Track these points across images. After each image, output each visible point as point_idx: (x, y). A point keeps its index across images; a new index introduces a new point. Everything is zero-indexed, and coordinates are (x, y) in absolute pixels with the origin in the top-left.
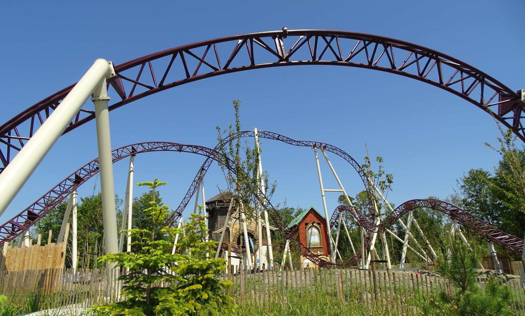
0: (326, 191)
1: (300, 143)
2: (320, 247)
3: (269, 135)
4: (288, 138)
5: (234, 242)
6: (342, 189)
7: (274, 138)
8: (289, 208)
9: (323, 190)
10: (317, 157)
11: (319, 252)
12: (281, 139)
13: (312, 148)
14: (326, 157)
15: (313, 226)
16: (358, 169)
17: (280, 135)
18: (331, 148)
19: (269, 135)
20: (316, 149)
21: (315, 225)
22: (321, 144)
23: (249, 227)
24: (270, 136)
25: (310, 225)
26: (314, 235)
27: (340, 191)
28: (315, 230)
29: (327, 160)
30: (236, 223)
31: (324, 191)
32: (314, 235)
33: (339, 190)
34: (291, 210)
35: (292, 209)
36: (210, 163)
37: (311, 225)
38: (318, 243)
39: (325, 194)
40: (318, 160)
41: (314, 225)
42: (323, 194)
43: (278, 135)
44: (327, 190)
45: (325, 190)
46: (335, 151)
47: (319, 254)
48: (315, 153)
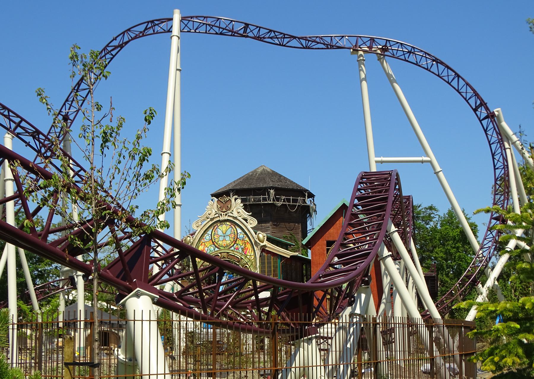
0: (382, 162)
1: (309, 41)
3: (219, 28)
4: (271, 31)
6: (427, 155)
7: (234, 33)
8: (423, 206)
10: (363, 76)
12: (251, 34)
13: (352, 53)
14: (388, 75)
16: (472, 101)
17: (247, 25)
19: (219, 28)
20: (361, 55)
22: (372, 40)
23: (233, 248)
24: (221, 30)
27: (422, 162)
29: (391, 83)
30: (203, 241)
31: (376, 162)
34: (429, 211)
35: (431, 208)
40: (364, 83)
43: (243, 26)
46: (412, 58)
48: (360, 66)
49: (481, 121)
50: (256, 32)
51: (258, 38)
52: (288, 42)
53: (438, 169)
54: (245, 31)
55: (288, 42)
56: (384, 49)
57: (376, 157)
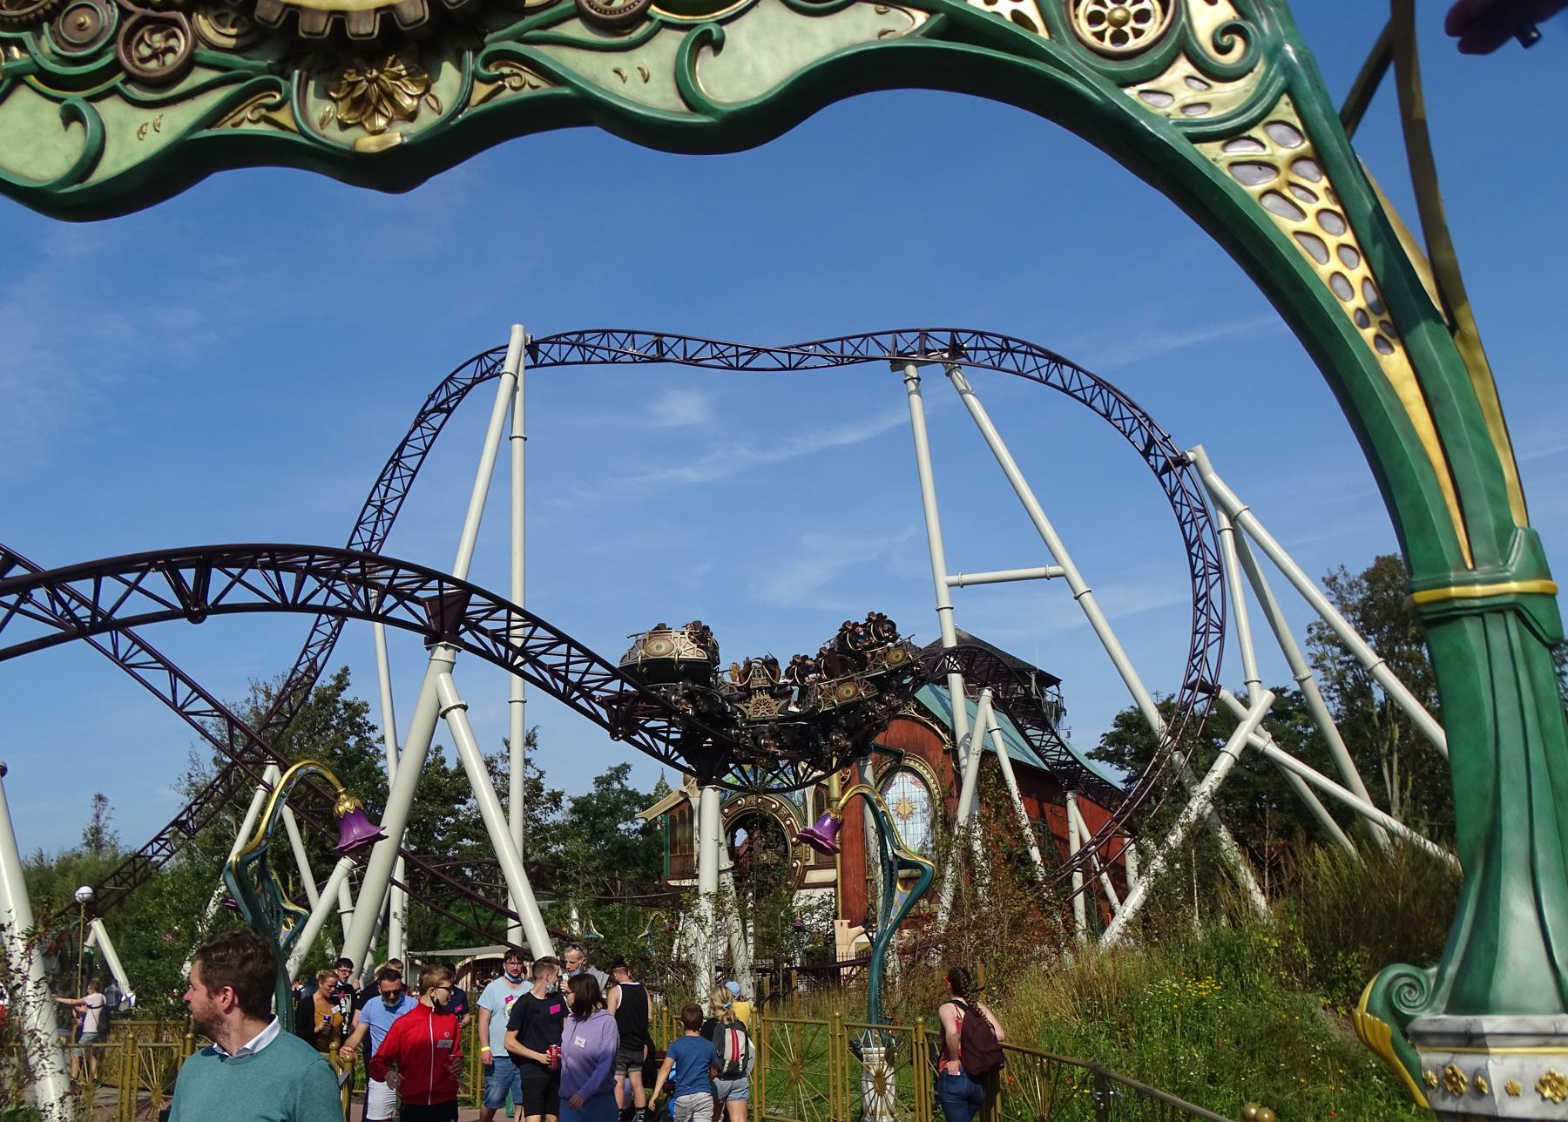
0: (962, 585)
6: (1058, 563)
9: (943, 579)
13: (893, 369)
18: (981, 344)
21: (912, 764)
31: (950, 585)
36: (387, 523)
39: (951, 595)
42: (945, 601)
44: (966, 578)
45: (954, 579)
49: (1159, 477)
50: (679, 350)
51: (689, 361)
52: (747, 363)
53: (1081, 587)
54: (660, 349)
55: (747, 363)
56: (956, 350)
57: (948, 575)
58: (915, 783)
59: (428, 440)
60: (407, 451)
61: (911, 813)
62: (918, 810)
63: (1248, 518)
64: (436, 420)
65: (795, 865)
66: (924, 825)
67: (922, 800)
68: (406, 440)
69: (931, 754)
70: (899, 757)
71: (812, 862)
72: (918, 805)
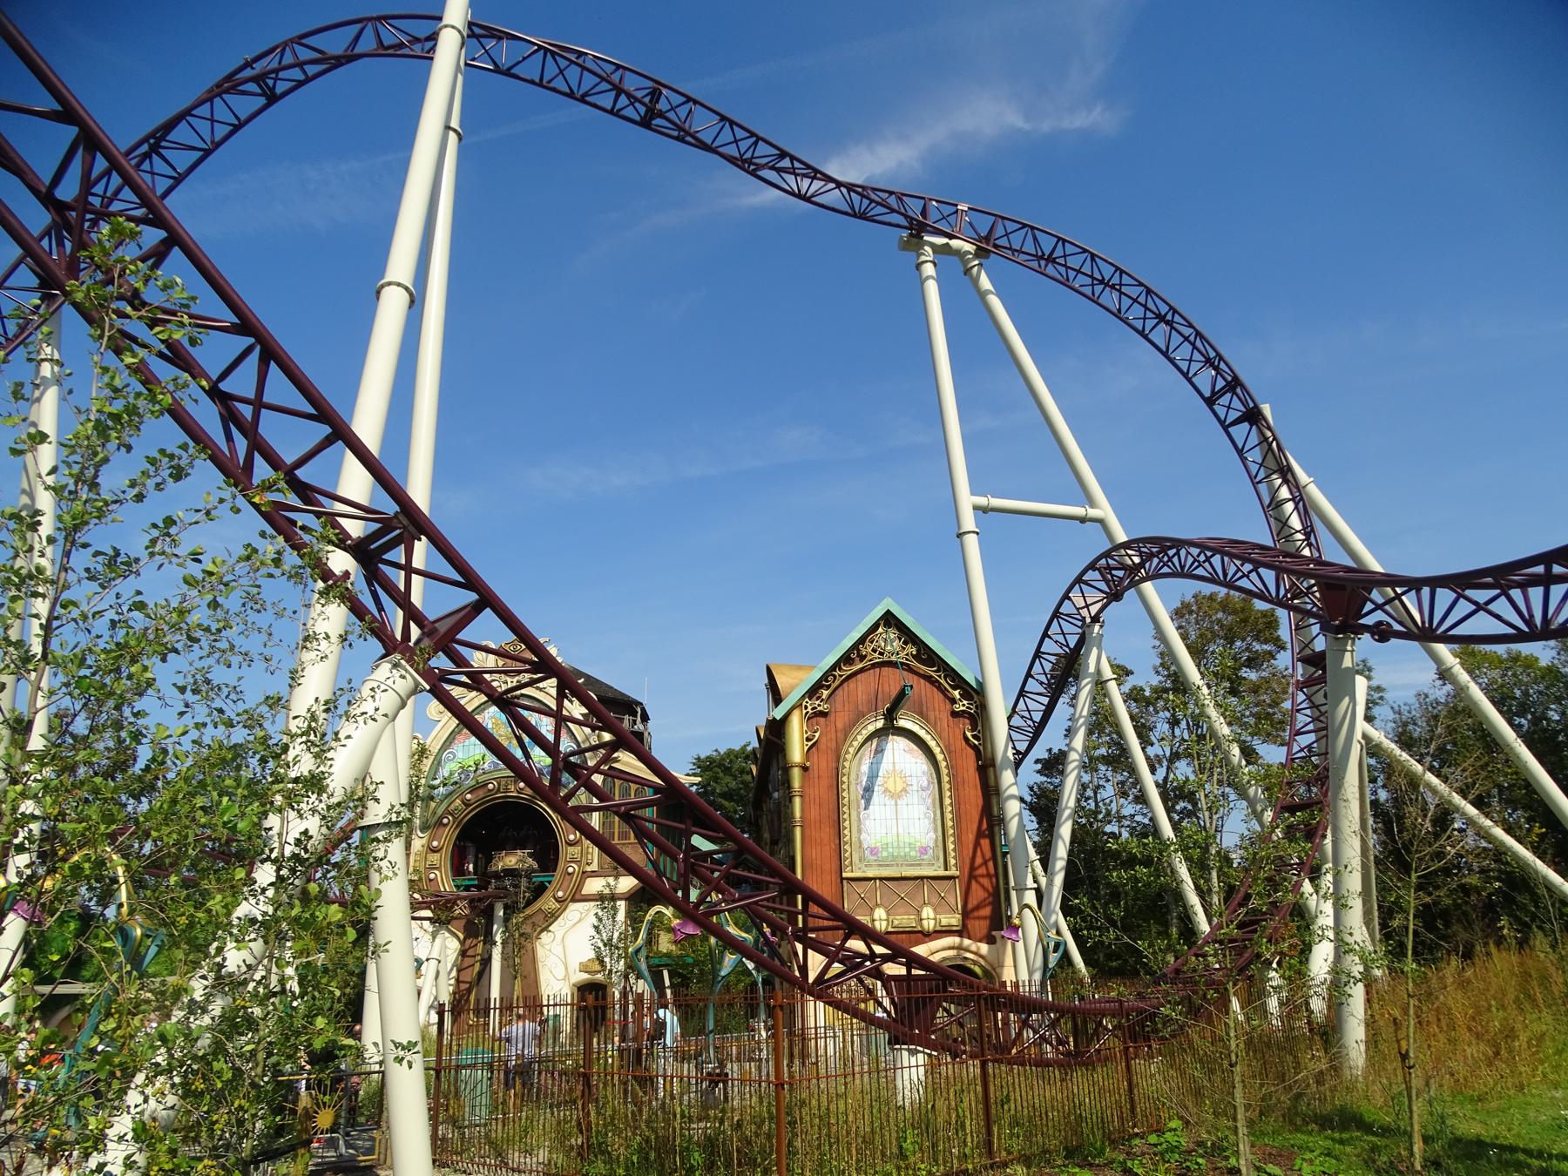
2: (942, 873)
5: (434, 858)
6: (1091, 502)
9: (967, 501)
11: (928, 912)
15: (890, 729)
25: (871, 728)
26: (895, 796)
27: (1083, 520)
28: (901, 757)
31: (976, 508)
32: (895, 796)
33: (1078, 511)
37: (880, 724)
38: (924, 850)
41: (902, 723)
42: (969, 521)
45: (982, 501)
47: (929, 925)
57: (973, 493)
58: (910, 751)
59: (221, 131)
60: (181, 133)
61: (904, 790)
62: (915, 788)
63: (1314, 491)
64: (245, 105)
65: (570, 870)
66: (923, 808)
67: (920, 774)
68: (188, 112)
69: (931, 715)
70: (890, 715)
71: (594, 867)
72: (914, 781)
